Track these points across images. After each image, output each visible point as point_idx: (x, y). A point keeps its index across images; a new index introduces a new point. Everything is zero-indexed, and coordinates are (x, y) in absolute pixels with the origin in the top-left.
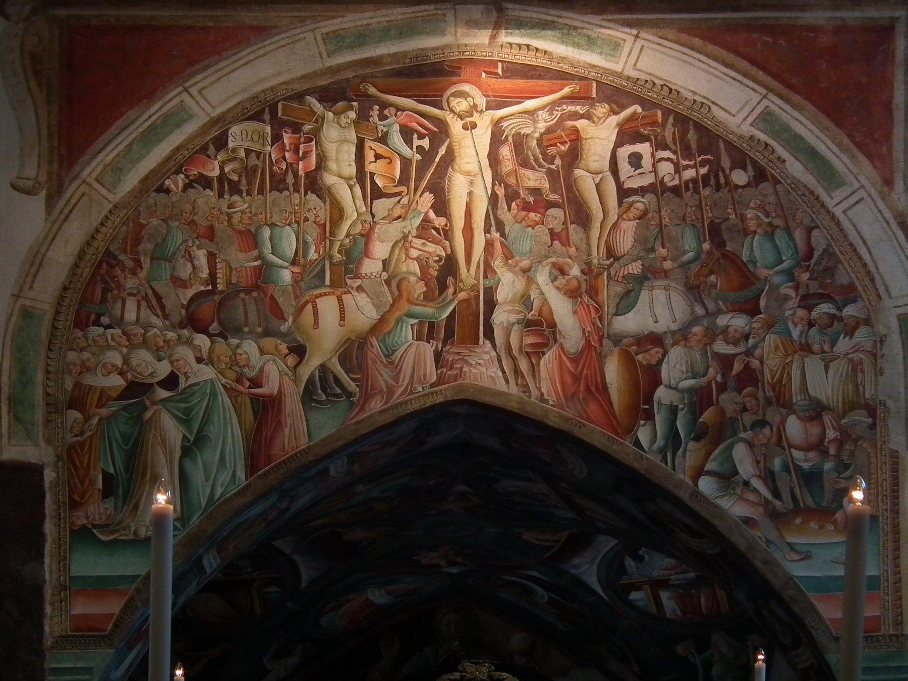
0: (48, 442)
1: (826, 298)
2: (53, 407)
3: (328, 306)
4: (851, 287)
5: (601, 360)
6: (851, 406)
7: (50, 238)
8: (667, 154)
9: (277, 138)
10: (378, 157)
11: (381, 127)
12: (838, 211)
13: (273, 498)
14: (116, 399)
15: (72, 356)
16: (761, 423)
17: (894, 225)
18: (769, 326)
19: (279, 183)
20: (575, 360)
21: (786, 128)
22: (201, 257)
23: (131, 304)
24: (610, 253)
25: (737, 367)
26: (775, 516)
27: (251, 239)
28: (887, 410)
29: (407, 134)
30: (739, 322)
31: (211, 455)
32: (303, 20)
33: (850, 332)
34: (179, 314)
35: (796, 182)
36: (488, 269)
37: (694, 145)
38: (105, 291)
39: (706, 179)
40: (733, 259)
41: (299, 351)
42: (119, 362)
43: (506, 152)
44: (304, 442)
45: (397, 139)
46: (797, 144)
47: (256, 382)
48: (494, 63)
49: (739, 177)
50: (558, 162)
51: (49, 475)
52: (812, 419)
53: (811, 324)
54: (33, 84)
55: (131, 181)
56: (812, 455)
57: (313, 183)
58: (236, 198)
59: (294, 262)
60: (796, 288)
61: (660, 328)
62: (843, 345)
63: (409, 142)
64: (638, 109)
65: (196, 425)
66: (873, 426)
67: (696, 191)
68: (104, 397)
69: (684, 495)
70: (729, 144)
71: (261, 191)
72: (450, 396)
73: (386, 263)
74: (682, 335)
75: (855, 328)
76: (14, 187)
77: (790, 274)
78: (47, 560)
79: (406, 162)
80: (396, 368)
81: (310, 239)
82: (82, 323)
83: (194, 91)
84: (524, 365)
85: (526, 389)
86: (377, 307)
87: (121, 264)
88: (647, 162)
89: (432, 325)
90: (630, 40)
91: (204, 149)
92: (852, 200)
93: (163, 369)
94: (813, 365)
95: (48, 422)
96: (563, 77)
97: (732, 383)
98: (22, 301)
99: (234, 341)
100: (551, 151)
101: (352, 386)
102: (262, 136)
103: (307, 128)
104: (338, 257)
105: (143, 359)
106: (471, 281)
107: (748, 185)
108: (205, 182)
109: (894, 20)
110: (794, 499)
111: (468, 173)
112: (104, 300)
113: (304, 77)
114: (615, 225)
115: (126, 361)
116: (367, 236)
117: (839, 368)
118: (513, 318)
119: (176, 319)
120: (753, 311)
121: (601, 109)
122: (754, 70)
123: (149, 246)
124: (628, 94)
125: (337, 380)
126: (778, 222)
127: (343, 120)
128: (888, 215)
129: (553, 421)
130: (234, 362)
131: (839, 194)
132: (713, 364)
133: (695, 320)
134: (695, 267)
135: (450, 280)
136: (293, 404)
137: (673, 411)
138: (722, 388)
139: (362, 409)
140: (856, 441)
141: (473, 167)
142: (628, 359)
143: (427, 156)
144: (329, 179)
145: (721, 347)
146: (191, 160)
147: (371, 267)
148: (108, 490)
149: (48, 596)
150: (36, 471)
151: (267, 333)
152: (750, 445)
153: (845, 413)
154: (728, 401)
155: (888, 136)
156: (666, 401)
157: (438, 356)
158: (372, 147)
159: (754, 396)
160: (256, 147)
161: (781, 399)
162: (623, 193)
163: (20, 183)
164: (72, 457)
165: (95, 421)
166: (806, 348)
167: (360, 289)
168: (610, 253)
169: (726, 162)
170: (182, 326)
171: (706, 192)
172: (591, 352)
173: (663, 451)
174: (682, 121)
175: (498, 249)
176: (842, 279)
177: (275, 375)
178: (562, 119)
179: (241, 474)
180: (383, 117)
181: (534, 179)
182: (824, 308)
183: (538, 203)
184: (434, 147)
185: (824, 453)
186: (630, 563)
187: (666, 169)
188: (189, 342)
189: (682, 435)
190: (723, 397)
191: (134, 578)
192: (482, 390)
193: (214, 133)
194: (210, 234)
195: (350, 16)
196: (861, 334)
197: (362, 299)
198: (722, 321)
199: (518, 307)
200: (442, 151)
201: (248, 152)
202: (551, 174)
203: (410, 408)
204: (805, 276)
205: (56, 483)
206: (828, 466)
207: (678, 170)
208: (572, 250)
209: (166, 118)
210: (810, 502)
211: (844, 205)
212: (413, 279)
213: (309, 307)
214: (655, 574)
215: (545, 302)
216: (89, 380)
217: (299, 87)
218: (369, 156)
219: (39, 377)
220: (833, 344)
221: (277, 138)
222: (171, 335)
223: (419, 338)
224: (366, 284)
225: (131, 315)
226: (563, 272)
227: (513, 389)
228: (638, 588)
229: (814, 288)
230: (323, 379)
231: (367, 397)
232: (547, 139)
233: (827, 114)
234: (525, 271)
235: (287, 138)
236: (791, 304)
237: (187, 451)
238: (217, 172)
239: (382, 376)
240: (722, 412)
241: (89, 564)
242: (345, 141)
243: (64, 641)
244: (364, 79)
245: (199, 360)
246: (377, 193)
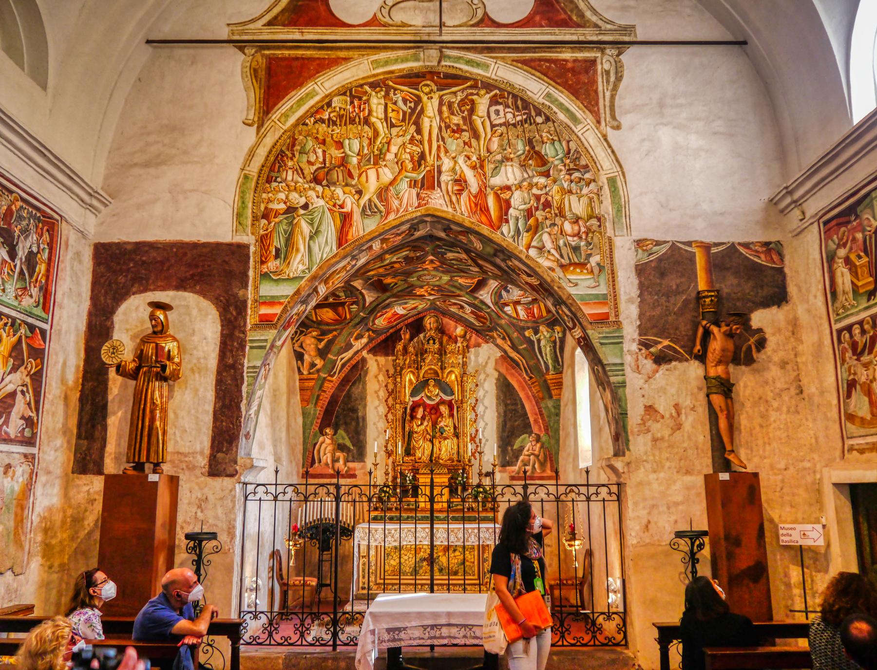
0: (253, 234)
1: (578, 170)
2: (255, 218)
3: (372, 173)
4: (586, 166)
5: (486, 196)
6: (590, 217)
7: (257, 145)
8: (510, 110)
9: (352, 103)
10: (393, 110)
11: (394, 98)
12: (579, 134)
13: (349, 259)
14: (283, 214)
15: (264, 196)
16: (554, 224)
17: (602, 139)
18: (555, 181)
19: (352, 121)
20: (475, 197)
21: (557, 100)
22: (320, 152)
23: (290, 172)
24: (488, 151)
25: (542, 200)
26: (562, 266)
27: (340, 145)
28: (605, 219)
29: (405, 101)
30: (542, 180)
31: (321, 239)
32: (363, 55)
33: (588, 184)
34: (309, 177)
35: (562, 123)
36: (439, 157)
37: (520, 107)
38: (280, 167)
39: (526, 120)
40: (538, 153)
41: (360, 193)
42: (284, 197)
43: (445, 108)
44: (361, 233)
45: (400, 103)
46: (561, 106)
47: (342, 207)
48: (439, 73)
49: (539, 120)
50: (466, 113)
51: (252, 249)
52: (574, 223)
53: (572, 182)
54: (254, 81)
55: (292, 120)
56: (575, 238)
57: (367, 121)
58: (335, 127)
59: (358, 155)
60: (565, 166)
61: (509, 183)
62: (585, 191)
63: (405, 104)
64: (498, 92)
65: (316, 226)
66: (600, 226)
67: (522, 125)
68: (277, 214)
69: (523, 257)
70: (534, 106)
71: (345, 125)
72: (423, 212)
73: (396, 155)
74: (519, 187)
75: (590, 183)
76: (244, 123)
77: (562, 160)
78: (250, 288)
79: (404, 113)
80: (401, 200)
81: (365, 145)
82: (269, 181)
83: (319, 83)
84: (454, 198)
85: (455, 209)
86: (393, 174)
87: (287, 155)
88: (502, 113)
89: (415, 181)
90: (493, 64)
91: (322, 107)
92: (585, 129)
93: (303, 201)
94: (574, 198)
95: (253, 225)
96: (467, 79)
97: (541, 207)
98: (244, 172)
99: (333, 189)
100: (463, 108)
101: (382, 208)
102: (346, 102)
103: (364, 98)
104: (376, 152)
105: (294, 196)
106: (431, 162)
107: (543, 123)
108: (323, 121)
109: (596, 58)
110: (569, 259)
111: (430, 117)
112: (279, 171)
113: (363, 78)
114: (490, 139)
115: (287, 198)
116: (389, 143)
117: (584, 200)
118: (449, 178)
119: (308, 179)
120: (547, 175)
121: (483, 92)
122: (542, 77)
123: (299, 148)
124: (493, 86)
125: (376, 206)
126: (556, 138)
127: (379, 95)
128: (600, 135)
129: (467, 224)
130: (332, 197)
131: (580, 127)
132: (533, 198)
133: (524, 180)
134: (523, 157)
135: (423, 162)
136: (357, 216)
137: (517, 219)
138: (537, 209)
139: (386, 218)
140: (593, 232)
141: (431, 115)
142: (497, 196)
143: (413, 110)
144: (373, 119)
145: (535, 191)
146: (317, 112)
147: (390, 156)
148: (277, 256)
149: (249, 306)
150: (246, 247)
151: (347, 185)
152: (550, 234)
153: (588, 220)
154: (540, 215)
155: (597, 104)
156: (514, 215)
157: (418, 195)
158: (390, 105)
159: (550, 212)
160: (343, 106)
161: (561, 214)
162: (493, 126)
163: (247, 121)
164: (264, 241)
165: (273, 224)
166: (570, 192)
167: (385, 166)
168: (488, 151)
169: (533, 114)
170: (311, 182)
171: (526, 126)
172: (481, 194)
173: (513, 237)
174: (515, 97)
175: (442, 149)
176: (583, 162)
177: (350, 204)
178: (467, 95)
179: (334, 248)
180: (395, 94)
181: (456, 120)
182: (577, 175)
183: (458, 130)
184: (416, 105)
185: (580, 238)
186: (504, 293)
187: (509, 116)
188: (314, 189)
189: (521, 229)
190: (537, 213)
191: (287, 296)
192: (436, 210)
193: (327, 100)
194: (324, 142)
195: (382, 54)
196: (592, 185)
197: (386, 170)
198: (535, 180)
199: (451, 173)
200: (419, 108)
201: (340, 108)
202: (463, 117)
203: (406, 218)
204: (568, 161)
205: (255, 253)
206: (583, 244)
207: (514, 117)
208: (473, 150)
209: (307, 95)
210: (576, 260)
211: (582, 131)
212: (407, 161)
213: (364, 174)
214: (515, 298)
215: (462, 171)
216: (271, 206)
217: (362, 82)
218: (390, 110)
219: (250, 205)
220: (581, 190)
221: (352, 103)
222: (306, 186)
223: (410, 187)
224: (388, 163)
225: (289, 178)
226: (469, 158)
227: (450, 210)
228: (508, 305)
229: (572, 166)
230: (370, 205)
231: (388, 213)
232: (462, 103)
233: (573, 94)
234: (454, 158)
235: (356, 103)
236: (563, 173)
237: (311, 238)
238: (327, 117)
239: (395, 203)
240: (537, 220)
241: (268, 290)
242: (380, 104)
243: (256, 327)
244: (387, 79)
245: (318, 197)
246: (393, 126)
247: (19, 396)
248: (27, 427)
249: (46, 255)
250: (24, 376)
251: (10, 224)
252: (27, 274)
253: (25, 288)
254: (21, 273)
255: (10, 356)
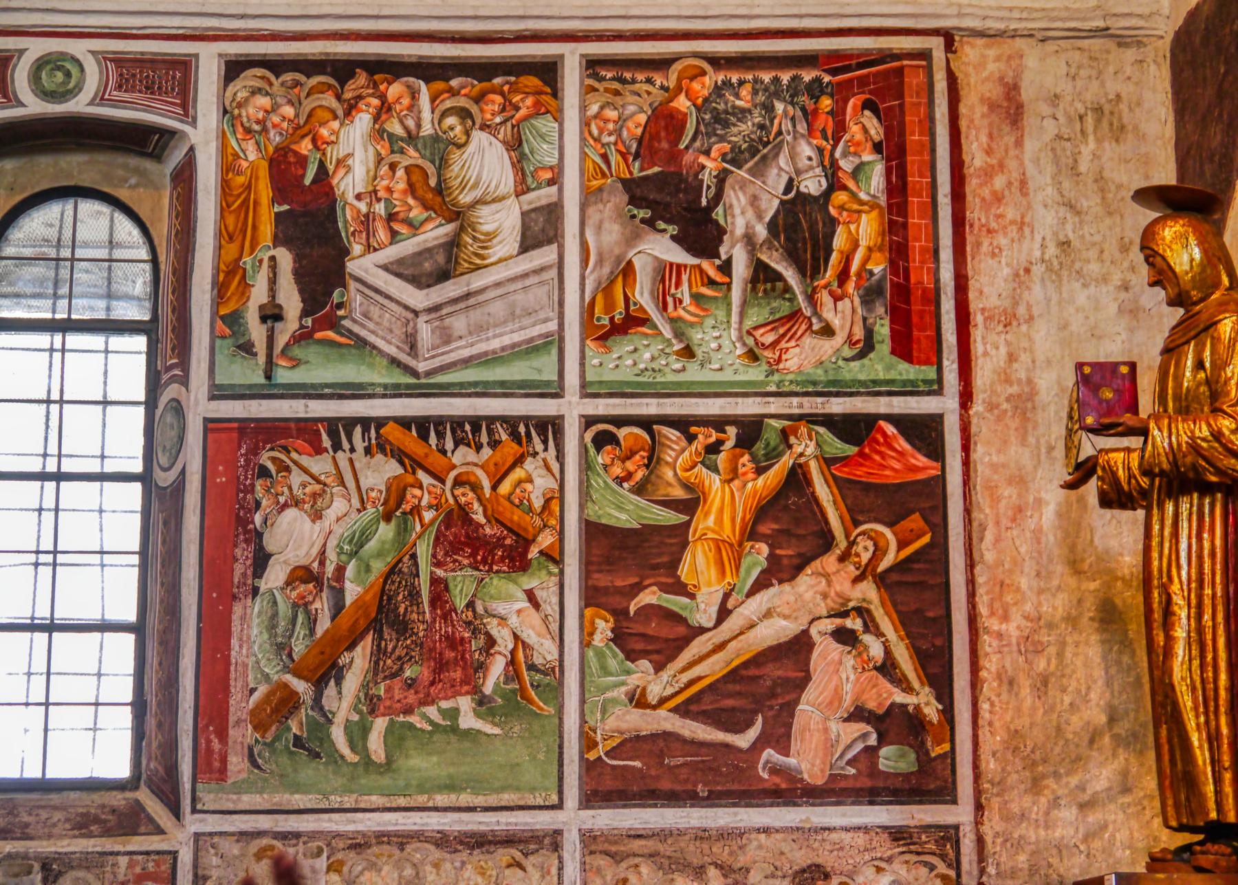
247: (826, 652)
248: (882, 740)
249: (876, 181)
250: (842, 584)
251: (674, 156)
252: (790, 275)
253: (795, 315)
254: (762, 275)
255: (751, 533)
